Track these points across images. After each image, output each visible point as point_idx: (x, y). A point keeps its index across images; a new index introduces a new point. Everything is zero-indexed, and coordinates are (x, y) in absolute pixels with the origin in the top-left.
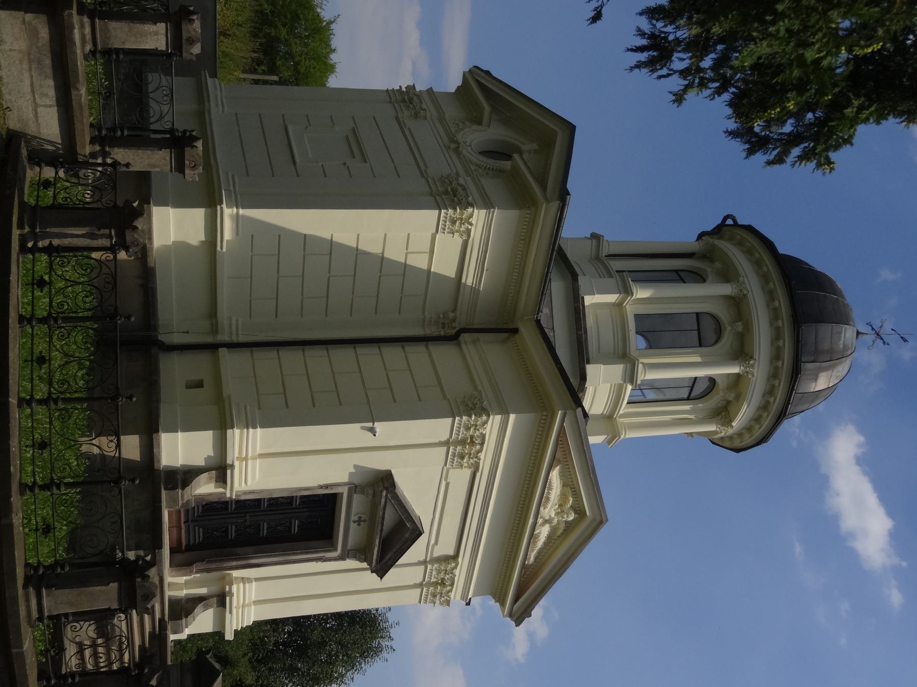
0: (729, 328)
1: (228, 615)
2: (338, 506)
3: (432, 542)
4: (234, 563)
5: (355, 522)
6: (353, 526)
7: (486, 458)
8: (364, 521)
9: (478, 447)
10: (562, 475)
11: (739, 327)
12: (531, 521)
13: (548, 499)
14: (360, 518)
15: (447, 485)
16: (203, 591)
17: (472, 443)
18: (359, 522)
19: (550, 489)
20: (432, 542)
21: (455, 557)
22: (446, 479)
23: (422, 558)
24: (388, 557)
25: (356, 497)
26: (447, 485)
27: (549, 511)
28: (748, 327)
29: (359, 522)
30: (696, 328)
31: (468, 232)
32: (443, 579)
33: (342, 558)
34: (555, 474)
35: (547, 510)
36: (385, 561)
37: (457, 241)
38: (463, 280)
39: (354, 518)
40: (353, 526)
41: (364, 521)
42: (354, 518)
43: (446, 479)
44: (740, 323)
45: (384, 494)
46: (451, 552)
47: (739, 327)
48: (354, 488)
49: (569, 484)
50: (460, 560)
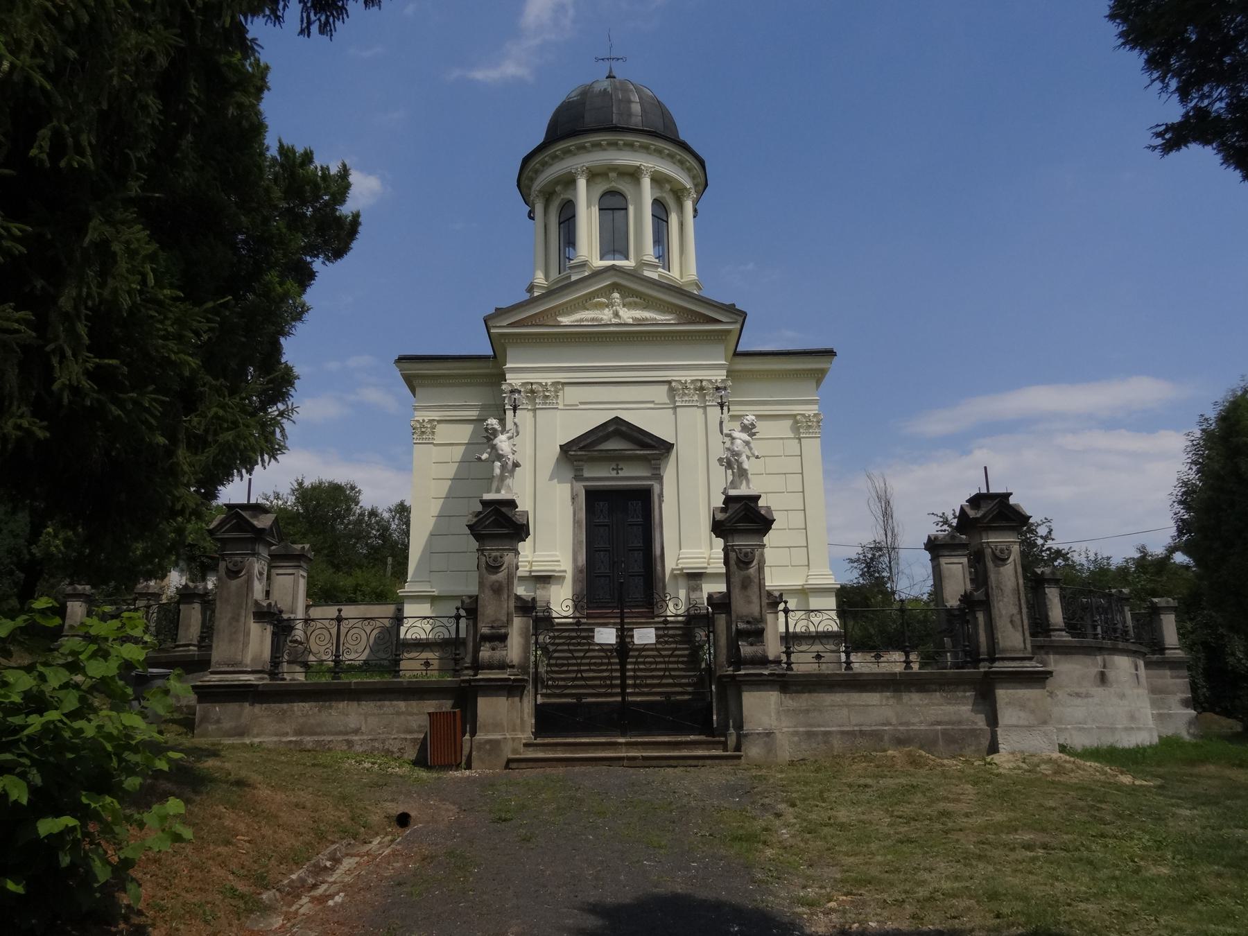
0: (613, 184)
1: (708, 571)
2: (605, 488)
3: (651, 405)
4: (659, 568)
5: (618, 473)
6: (621, 474)
7: (548, 379)
8: (617, 465)
9: (534, 387)
10: (561, 314)
11: (613, 175)
12: (612, 329)
13: (593, 320)
14: (613, 469)
15: (581, 403)
16: (682, 594)
17: (532, 391)
18: (617, 469)
19: (582, 320)
20: (651, 405)
21: (669, 382)
22: (577, 405)
23: (671, 411)
24: (650, 441)
25: (586, 474)
26: (581, 403)
27: (606, 315)
28: (615, 168)
29: (617, 469)
30: (611, 212)
31: (431, 421)
32: (696, 389)
33: (660, 479)
34: (565, 320)
35: (604, 317)
36: (654, 443)
37: (440, 428)
38: (474, 418)
39: (614, 474)
40: (621, 474)
41: (617, 465)
42: (614, 474)
43: (577, 405)
44: (610, 175)
45: (573, 453)
46: (665, 388)
47: (613, 175)
48: (578, 478)
49: (583, 303)
50: (669, 379)
